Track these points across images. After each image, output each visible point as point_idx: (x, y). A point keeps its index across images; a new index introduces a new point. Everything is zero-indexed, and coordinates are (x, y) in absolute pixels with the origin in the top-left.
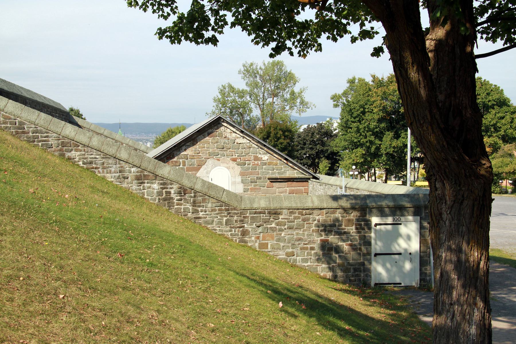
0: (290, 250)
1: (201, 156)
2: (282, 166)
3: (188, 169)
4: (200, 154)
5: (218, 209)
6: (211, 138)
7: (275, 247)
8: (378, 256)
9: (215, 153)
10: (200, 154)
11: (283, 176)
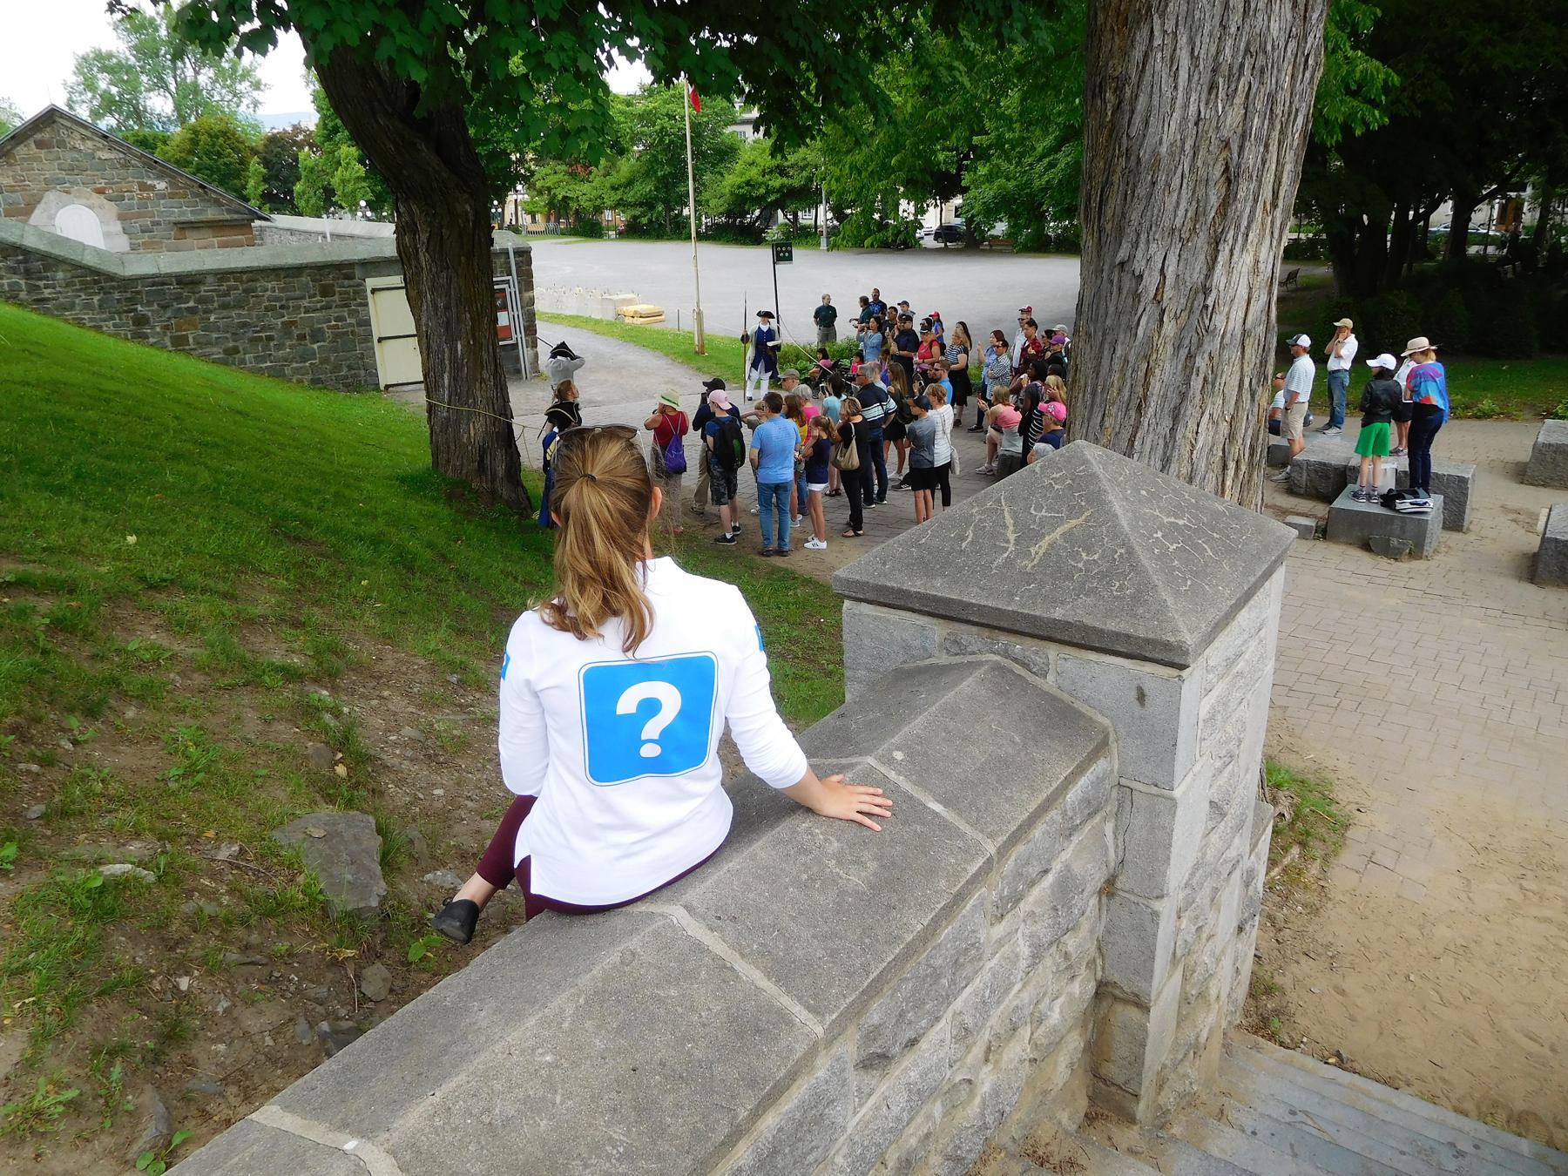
0: (231, 344)
5: (79, 281)
6: (43, 151)
7: (201, 340)
8: (383, 342)
9: (58, 179)
11: (202, 217)
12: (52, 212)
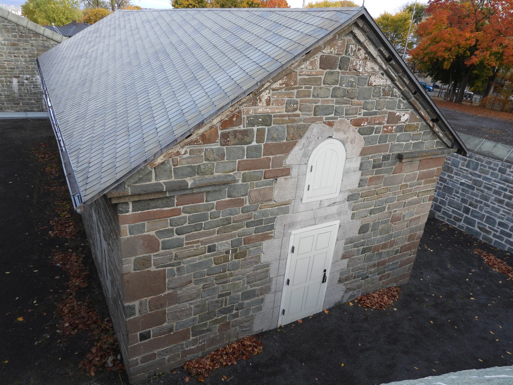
1: (298, 115)
3: (268, 150)
4: (298, 112)
6: (325, 71)
10: (298, 112)
12: (310, 148)
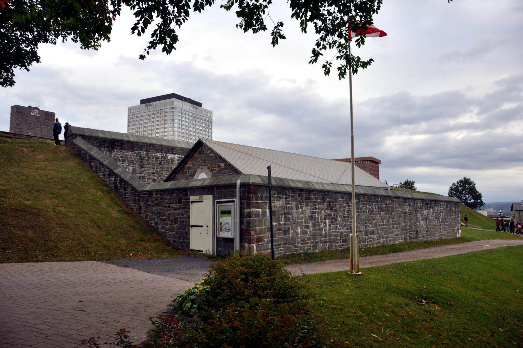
0: (156, 220)
2: (231, 170)
